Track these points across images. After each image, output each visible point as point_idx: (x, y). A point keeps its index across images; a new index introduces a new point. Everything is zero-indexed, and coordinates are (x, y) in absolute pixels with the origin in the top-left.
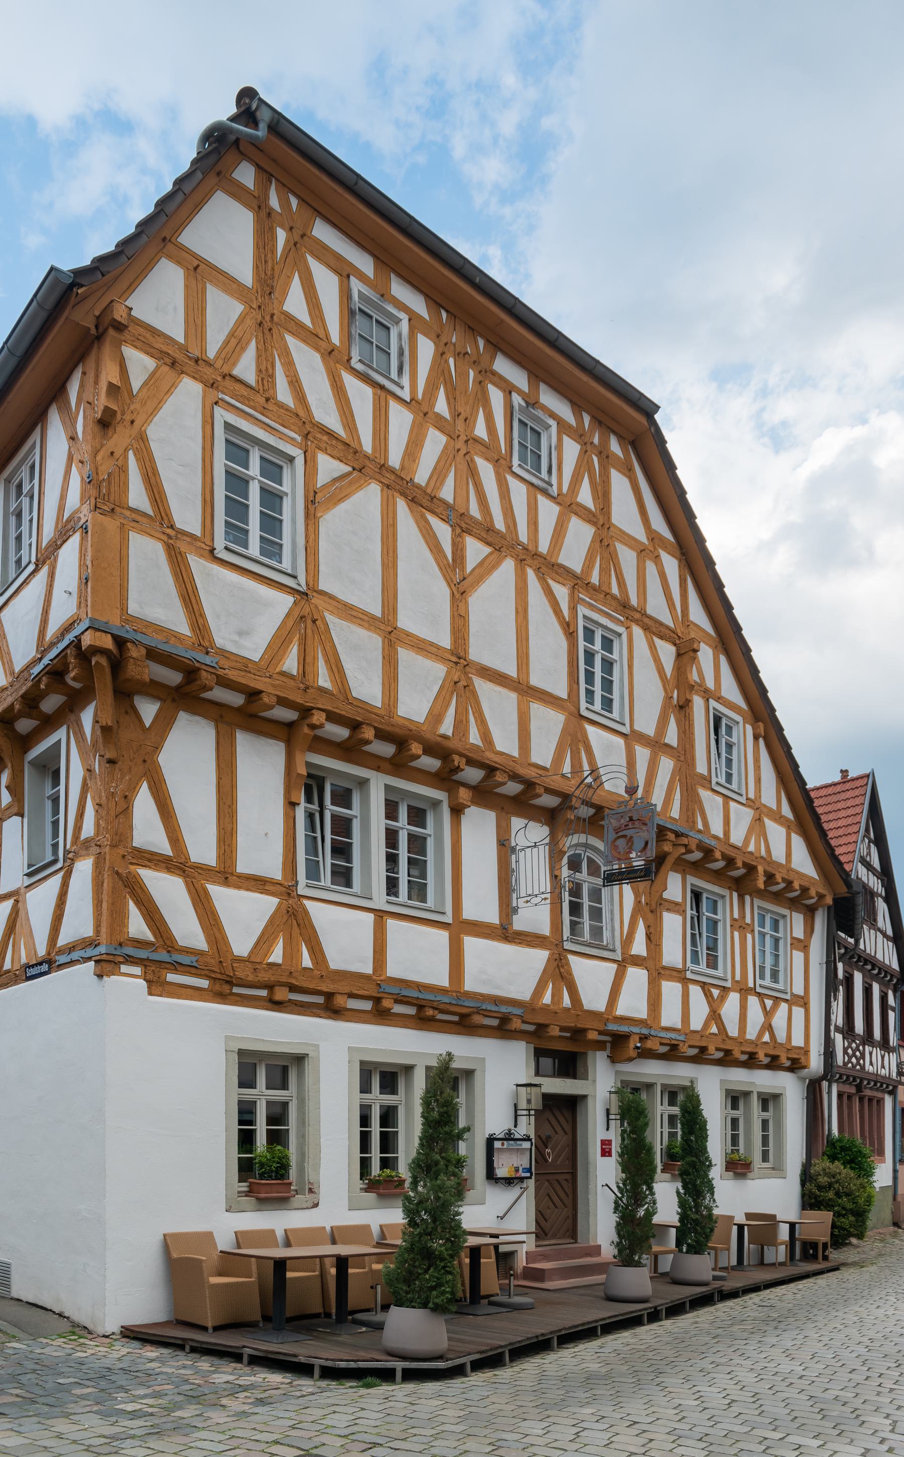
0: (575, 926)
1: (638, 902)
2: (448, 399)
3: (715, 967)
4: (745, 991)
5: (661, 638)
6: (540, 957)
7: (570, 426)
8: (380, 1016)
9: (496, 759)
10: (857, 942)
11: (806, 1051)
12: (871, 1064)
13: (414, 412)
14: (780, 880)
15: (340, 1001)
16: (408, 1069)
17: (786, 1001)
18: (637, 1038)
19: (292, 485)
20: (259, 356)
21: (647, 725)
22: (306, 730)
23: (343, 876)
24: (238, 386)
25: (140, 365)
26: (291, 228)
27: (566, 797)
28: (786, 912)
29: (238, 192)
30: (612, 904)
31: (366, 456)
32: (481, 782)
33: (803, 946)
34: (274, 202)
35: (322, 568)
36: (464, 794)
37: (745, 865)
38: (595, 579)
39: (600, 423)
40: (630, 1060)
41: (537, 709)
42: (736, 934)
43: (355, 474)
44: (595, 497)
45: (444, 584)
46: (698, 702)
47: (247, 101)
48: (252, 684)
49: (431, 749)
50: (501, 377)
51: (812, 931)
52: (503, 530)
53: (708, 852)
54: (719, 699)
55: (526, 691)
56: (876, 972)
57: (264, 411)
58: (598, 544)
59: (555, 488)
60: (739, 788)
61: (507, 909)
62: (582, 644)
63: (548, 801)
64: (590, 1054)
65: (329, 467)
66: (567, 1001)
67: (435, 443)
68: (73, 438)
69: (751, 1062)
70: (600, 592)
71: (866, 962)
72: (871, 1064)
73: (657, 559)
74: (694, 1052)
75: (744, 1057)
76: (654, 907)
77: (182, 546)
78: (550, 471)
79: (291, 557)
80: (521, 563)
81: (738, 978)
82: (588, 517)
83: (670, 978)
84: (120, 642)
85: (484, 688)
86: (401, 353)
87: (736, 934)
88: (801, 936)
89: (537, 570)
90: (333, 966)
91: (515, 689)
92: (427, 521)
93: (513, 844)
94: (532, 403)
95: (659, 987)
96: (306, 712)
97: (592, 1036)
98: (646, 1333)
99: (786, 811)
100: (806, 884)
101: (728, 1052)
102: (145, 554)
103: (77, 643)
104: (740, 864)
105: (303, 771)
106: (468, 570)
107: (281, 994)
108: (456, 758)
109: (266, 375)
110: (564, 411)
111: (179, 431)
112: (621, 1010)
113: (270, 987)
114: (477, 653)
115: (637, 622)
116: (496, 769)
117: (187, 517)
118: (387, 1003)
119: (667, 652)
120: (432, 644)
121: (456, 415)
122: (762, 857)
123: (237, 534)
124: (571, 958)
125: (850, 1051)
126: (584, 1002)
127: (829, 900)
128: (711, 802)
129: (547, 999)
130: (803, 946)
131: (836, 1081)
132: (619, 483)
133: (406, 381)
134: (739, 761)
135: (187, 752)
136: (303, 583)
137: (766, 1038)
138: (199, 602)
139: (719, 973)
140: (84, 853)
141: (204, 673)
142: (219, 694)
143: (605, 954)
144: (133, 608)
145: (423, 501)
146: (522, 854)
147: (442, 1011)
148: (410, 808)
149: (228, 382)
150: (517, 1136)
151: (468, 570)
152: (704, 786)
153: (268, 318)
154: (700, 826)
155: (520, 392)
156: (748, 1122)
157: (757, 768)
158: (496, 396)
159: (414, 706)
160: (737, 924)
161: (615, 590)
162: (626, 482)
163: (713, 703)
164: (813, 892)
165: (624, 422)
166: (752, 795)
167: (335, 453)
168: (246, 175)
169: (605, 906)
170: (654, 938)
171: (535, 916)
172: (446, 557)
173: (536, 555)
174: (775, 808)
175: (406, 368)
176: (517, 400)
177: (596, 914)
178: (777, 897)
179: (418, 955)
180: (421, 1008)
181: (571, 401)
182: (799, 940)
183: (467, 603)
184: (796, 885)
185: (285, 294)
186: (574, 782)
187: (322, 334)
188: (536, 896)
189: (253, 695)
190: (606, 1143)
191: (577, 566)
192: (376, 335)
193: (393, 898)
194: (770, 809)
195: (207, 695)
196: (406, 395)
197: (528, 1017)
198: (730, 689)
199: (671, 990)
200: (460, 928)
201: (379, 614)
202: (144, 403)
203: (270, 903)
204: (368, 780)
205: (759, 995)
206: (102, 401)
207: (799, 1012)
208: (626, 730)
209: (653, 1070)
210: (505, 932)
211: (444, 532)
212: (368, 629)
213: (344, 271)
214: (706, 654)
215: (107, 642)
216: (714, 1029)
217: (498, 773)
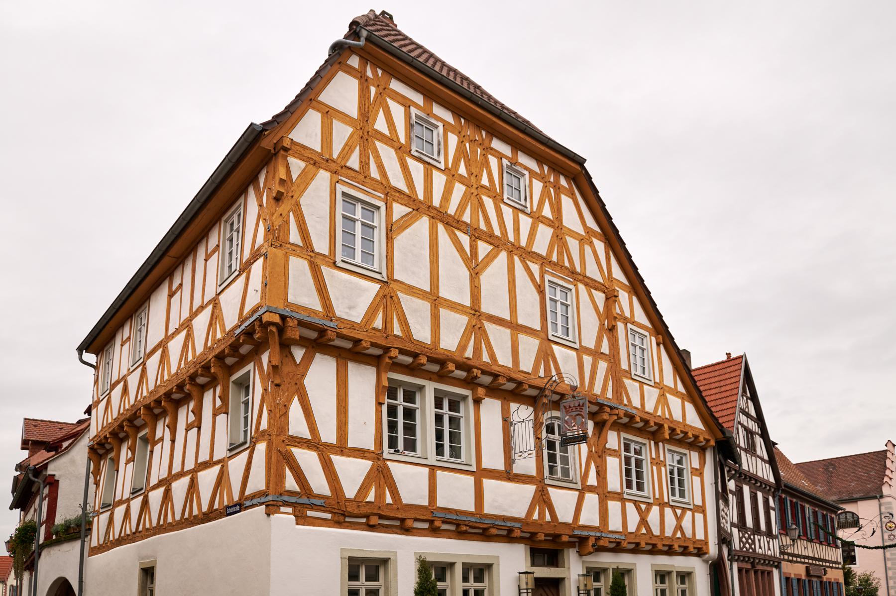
0: (552, 469)
1: (590, 451)
2: (466, 166)
3: (643, 490)
4: (662, 505)
5: (596, 289)
6: (530, 490)
7: (536, 173)
8: (434, 531)
11: (706, 542)
15: (409, 523)
16: (452, 565)
17: (690, 510)
18: (593, 539)
20: (361, 154)
21: (589, 342)
22: (387, 360)
23: (411, 445)
24: (349, 171)
25: (297, 165)
27: (542, 390)
28: (686, 451)
31: (420, 202)
33: (699, 472)
35: (395, 267)
36: (481, 391)
37: (656, 424)
38: (554, 258)
39: (554, 170)
40: (590, 553)
41: (523, 338)
42: (655, 468)
44: (553, 211)
46: (620, 326)
48: (357, 336)
49: (459, 366)
50: (496, 151)
51: (705, 463)
52: (499, 235)
53: (632, 417)
54: (633, 323)
59: (529, 209)
62: (548, 296)
65: (399, 210)
66: (548, 517)
67: (459, 190)
69: (670, 551)
70: (558, 265)
73: (591, 244)
74: (632, 546)
75: (666, 548)
77: (318, 261)
78: (526, 200)
80: (510, 253)
81: (657, 496)
82: (549, 223)
83: (613, 499)
84: (283, 318)
85: (489, 327)
86: (439, 144)
87: (655, 468)
90: (405, 502)
91: (509, 327)
92: (455, 235)
94: (514, 162)
95: (607, 504)
96: (387, 349)
97: (565, 539)
99: (681, 388)
100: (697, 434)
101: (654, 545)
104: (652, 424)
105: (386, 383)
106: (480, 259)
107: (374, 520)
108: (475, 370)
109: (364, 164)
110: (533, 165)
111: (317, 198)
112: (582, 521)
113: (367, 517)
114: (486, 307)
115: (581, 281)
117: (321, 245)
118: (437, 523)
119: (600, 297)
120: (459, 305)
121: (471, 174)
124: (549, 489)
126: (559, 517)
127: (713, 443)
128: (632, 387)
129: (536, 516)
130: (699, 472)
132: (566, 202)
133: (442, 159)
136: (385, 276)
137: (679, 535)
139: (645, 494)
142: (338, 342)
143: (571, 486)
145: (453, 223)
147: (471, 527)
149: (344, 170)
152: (627, 377)
154: (626, 402)
155: (507, 158)
156: (671, 592)
157: (660, 363)
158: (493, 161)
159: (449, 342)
161: (567, 264)
162: (571, 200)
163: (629, 326)
164: (701, 439)
165: (567, 168)
166: (657, 380)
167: (403, 202)
169: (570, 454)
170: (601, 474)
171: (526, 465)
173: (519, 248)
175: (442, 152)
176: (505, 162)
177: (565, 460)
179: (456, 493)
180: (458, 525)
181: (536, 159)
184: (690, 435)
185: (375, 120)
186: (546, 380)
191: (544, 253)
192: (426, 135)
193: (440, 458)
195: (332, 343)
196: (442, 166)
197: (525, 529)
198: (640, 316)
199: (614, 506)
200: (481, 474)
201: (428, 290)
202: (298, 186)
203: (367, 464)
204: (424, 386)
205: (672, 507)
206: (276, 188)
207: (699, 517)
208: (577, 346)
209: (607, 560)
210: (508, 475)
211: (465, 239)
213: (407, 104)
214: (624, 296)
215: (276, 319)
216: (644, 531)
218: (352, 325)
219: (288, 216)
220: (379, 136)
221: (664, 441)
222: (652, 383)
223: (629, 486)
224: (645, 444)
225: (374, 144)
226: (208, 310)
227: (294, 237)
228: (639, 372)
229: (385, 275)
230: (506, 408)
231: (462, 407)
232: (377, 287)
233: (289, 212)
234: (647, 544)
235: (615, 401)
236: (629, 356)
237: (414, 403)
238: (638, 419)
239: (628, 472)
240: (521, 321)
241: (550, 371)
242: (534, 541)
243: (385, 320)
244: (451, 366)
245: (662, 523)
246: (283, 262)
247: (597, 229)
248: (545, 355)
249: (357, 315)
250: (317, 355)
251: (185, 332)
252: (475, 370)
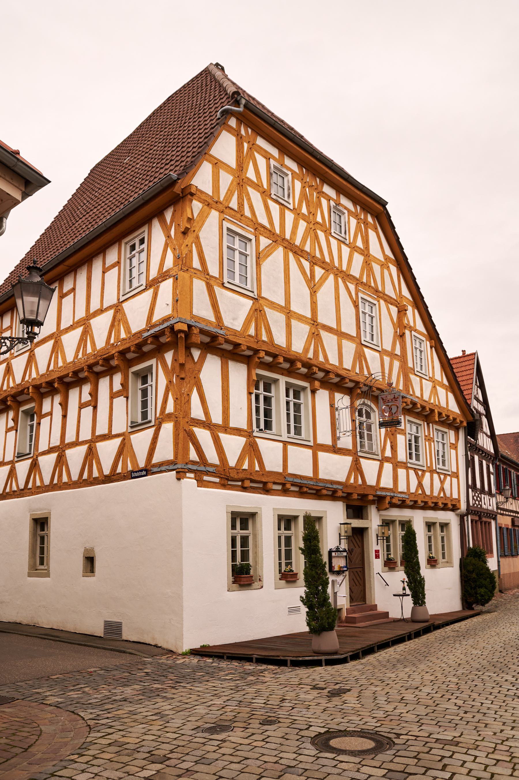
6: (348, 460)
9: (330, 367)
13: (294, 214)
14: (444, 416)
18: (389, 498)
20: (238, 197)
26: (249, 142)
27: (357, 383)
28: (446, 430)
29: (230, 130)
30: (376, 432)
32: (322, 378)
34: (243, 132)
36: (317, 384)
40: (386, 509)
41: (345, 343)
43: (274, 243)
45: (308, 289)
47: (236, 96)
53: (414, 404)
55: (341, 335)
56: (484, 455)
60: (426, 372)
61: (335, 438)
63: (351, 385)
64: (369, 506)
66: (360, 482)
68: (168, 236)
71: (479, 449)
76: (393, 432)
85: (324, 334)
88: (454, 442)
91: (336, 334)
92: (300, 261)
93: (336, 406)
95: (397, 471)
97: (371, 498)
99: (445, 382)
100: (455, 417)
106: (316, 281)
108: (314, 368)
109: (241, 205)
112: (382, 485)
114: (321, 319)
116: (330, 372)
120: (304, 316)
122: (437, 405)
124: (361, 459)
126: (367, 481)
127: (465, 424)
129: (352, 481)
134: (425, 360)
140: (167, 419)
145: (299, 252)
148: (294, 391)
150: (341, 550)
151: (316, 281)
153: (241, 181)
154: (411, 393)
164: (458, 421)
166: (431, 376)
167: (266, 235)
168: (233, 122)
170: (394, 448)
171: (346, 442)
172: (308, 276)
174: (440, 380)
178: (442, 423)
183: (316, 296)
184: (451, 418)
185: (247, 170)
187: (260, 185)
188: (348, 432)
190: (377, 551)
194: (439, 381)
199: (402, 472)
204: (278, 380)
210: (334, 449)
211: (306, 265)
217: (331, 374)
218: (235, 333)
219: (192, 247)
220: (250, 183)
221: (436, 423)
222: (427, 378)
224: (420, 425)
225: (247, 189)
227: (196, 264)
228: (419, 369)
230: (332, 396)
231: (302, 395)
233: (192, 243)
235: (405, 392)
237: (270, 392)
238: (419, 406)
240: (344, 329)
242: (349, 500)
244: (299, 365)
246: (188, 283)
248: (360, 357)
249: (238, 326)
252: (314, 368)
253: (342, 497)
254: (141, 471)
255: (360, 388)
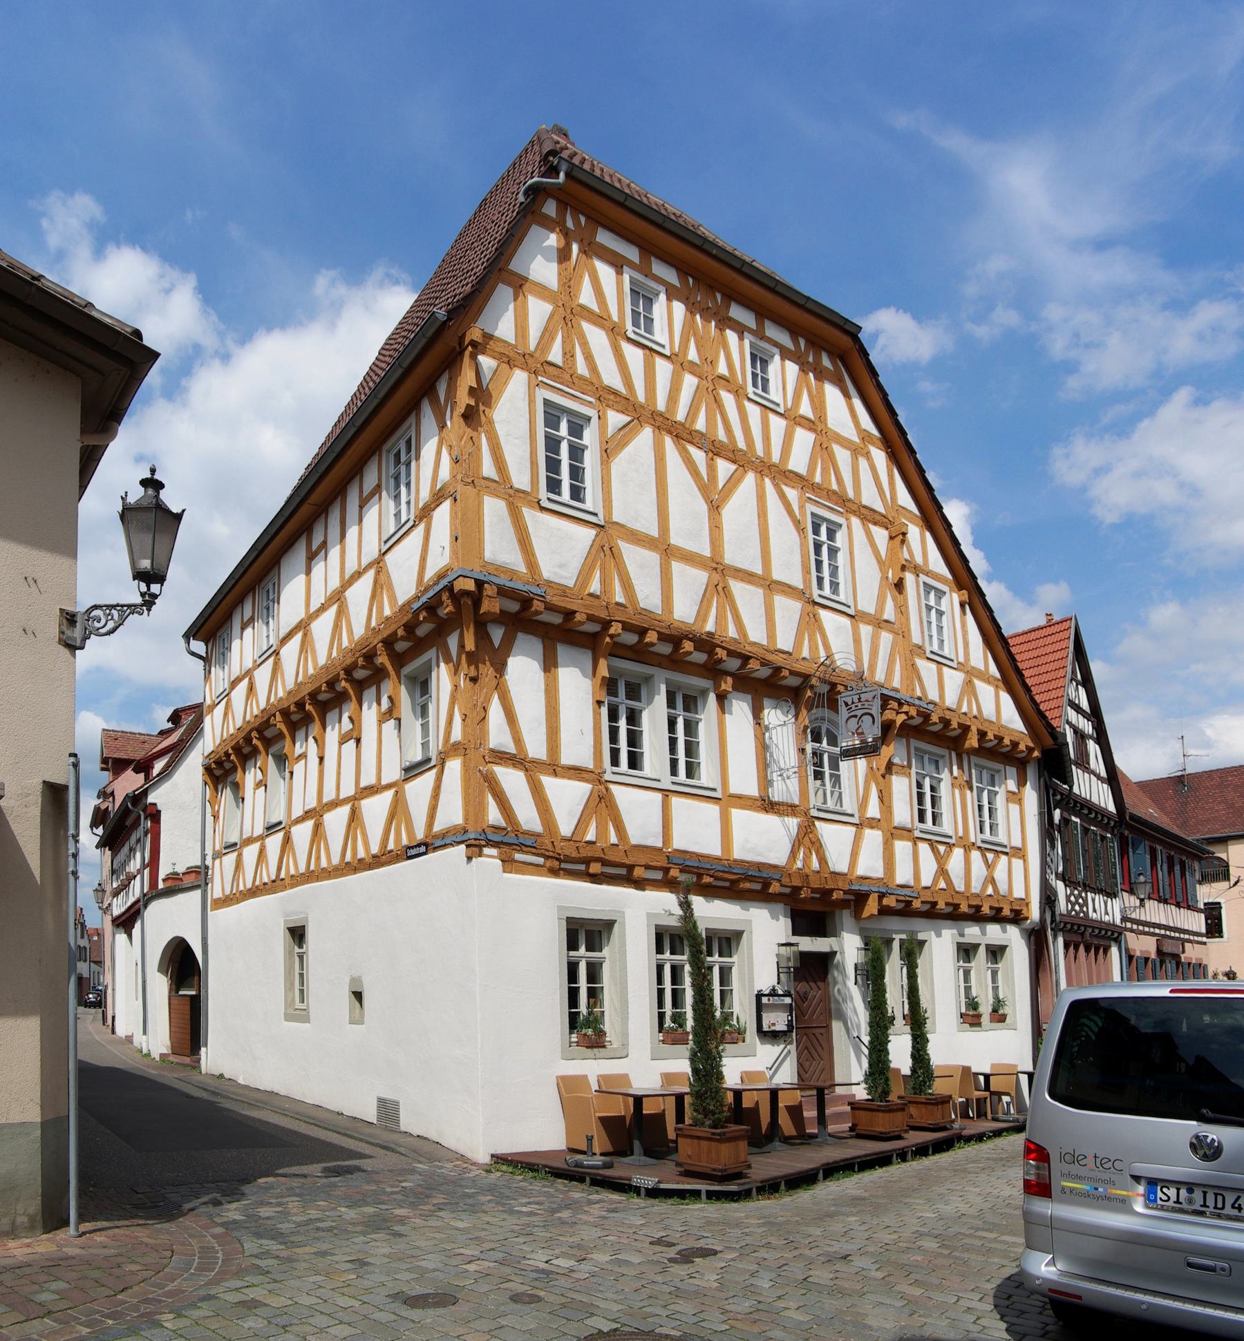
4: (968, 847)
5: (875, 524)
10: (1071, 787)
12: (1095, 911)
19: (590, 437)
22: (608, 639)
27: (806, 677)
28: (1001, 767)
38: (818, 479)
41: (780, 601)
44: (814, 408)
46: (909, 578)
48: (569, 606)
55: (771, 586)
56: (1093, 816)
57: (572, 385)
58: (818, 448)
64: (837, 912)
65: (615, 419)
66: (815, 864)
71: (1083, 806)
72: (1095, 911)
74: (927, 907)
79: (592, 500)
82: (809, 424)
83: (901, 838)
84: (480, 584)
85: (737, 587)
89: (773, 479)
91: (761, 586)
92: (687, 451)
98: (896, 1170)
99: (993, 669)
101: (956, 906)
102: (494, 509)
103: (449, 588)
108: (718, 650)
111: (514, 410)
112: (861, 871)
115: (854, 512)
117: (520, 478)
119: (880, 535)
123: (554, 486)
125: (1072, 898)
128: (927, 669)
131: (1061, 930)
135: (523, 669)
138: (531, 544)
141: (535, 602)
142: (547, 617)
144: (488, 555)
146: (774, 732)
159: (684, 611)
160: (957, 782)
170: (885, 799)
173: (771, 467)
182: (1014, 793)
189: (569, 614)
197: (785, 881)
203: (580, 791)
207: (1017, 863)
208: (851, 611)
212: (650, 549)
214: (914, 532)
215: (470, 586)
216: (942, 885)
223: (922, 819)
226: (370, 576)
228: (935, 648)
229: (601, 516)
232: (592, 533)
234: (947, 904)
236: (921, 623)
239: (921, 797)
240: (776, 576)
241: (817, 648)
243: (605, 582)
245: (967, 873)
247: (875, 432)
250: (520, 635)
251: (335, 607)
252: (718, 650)
253: (781, 894)
254: (419, 845)
255: (812, 687)
